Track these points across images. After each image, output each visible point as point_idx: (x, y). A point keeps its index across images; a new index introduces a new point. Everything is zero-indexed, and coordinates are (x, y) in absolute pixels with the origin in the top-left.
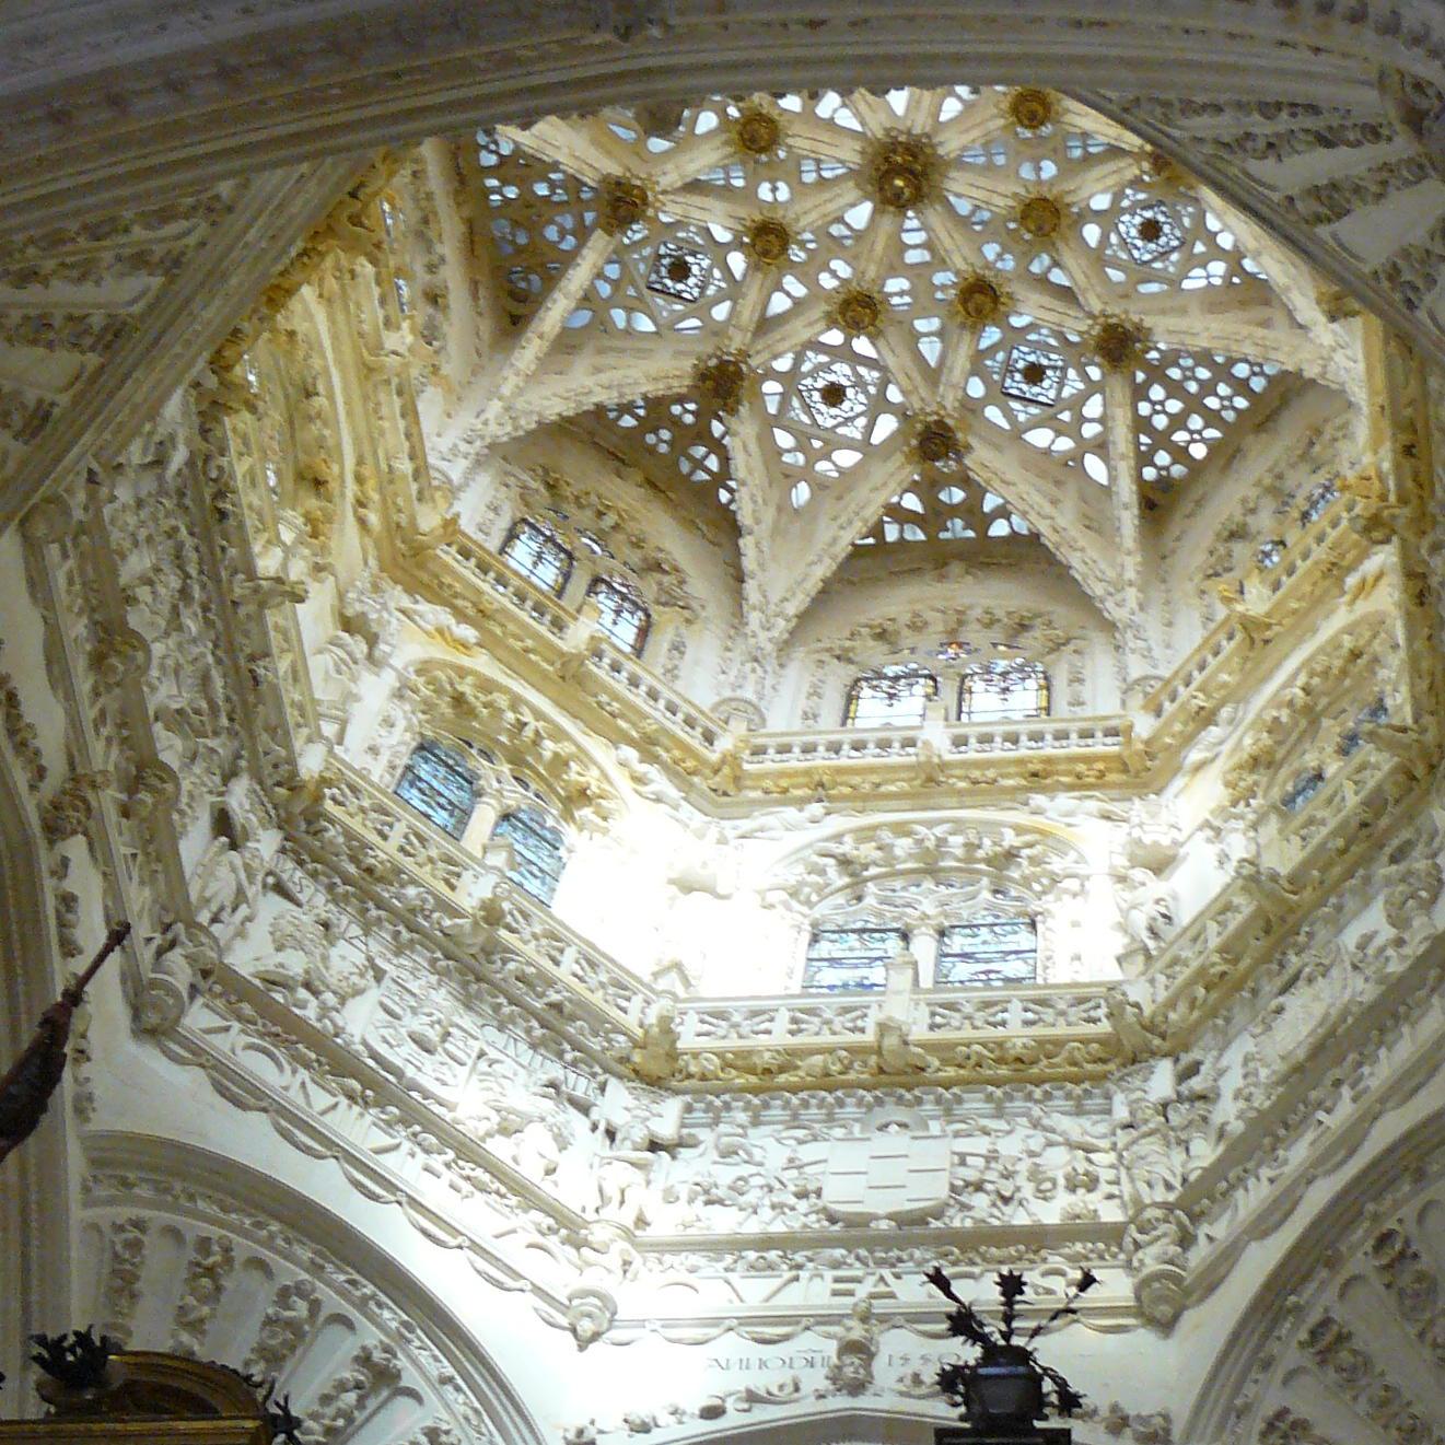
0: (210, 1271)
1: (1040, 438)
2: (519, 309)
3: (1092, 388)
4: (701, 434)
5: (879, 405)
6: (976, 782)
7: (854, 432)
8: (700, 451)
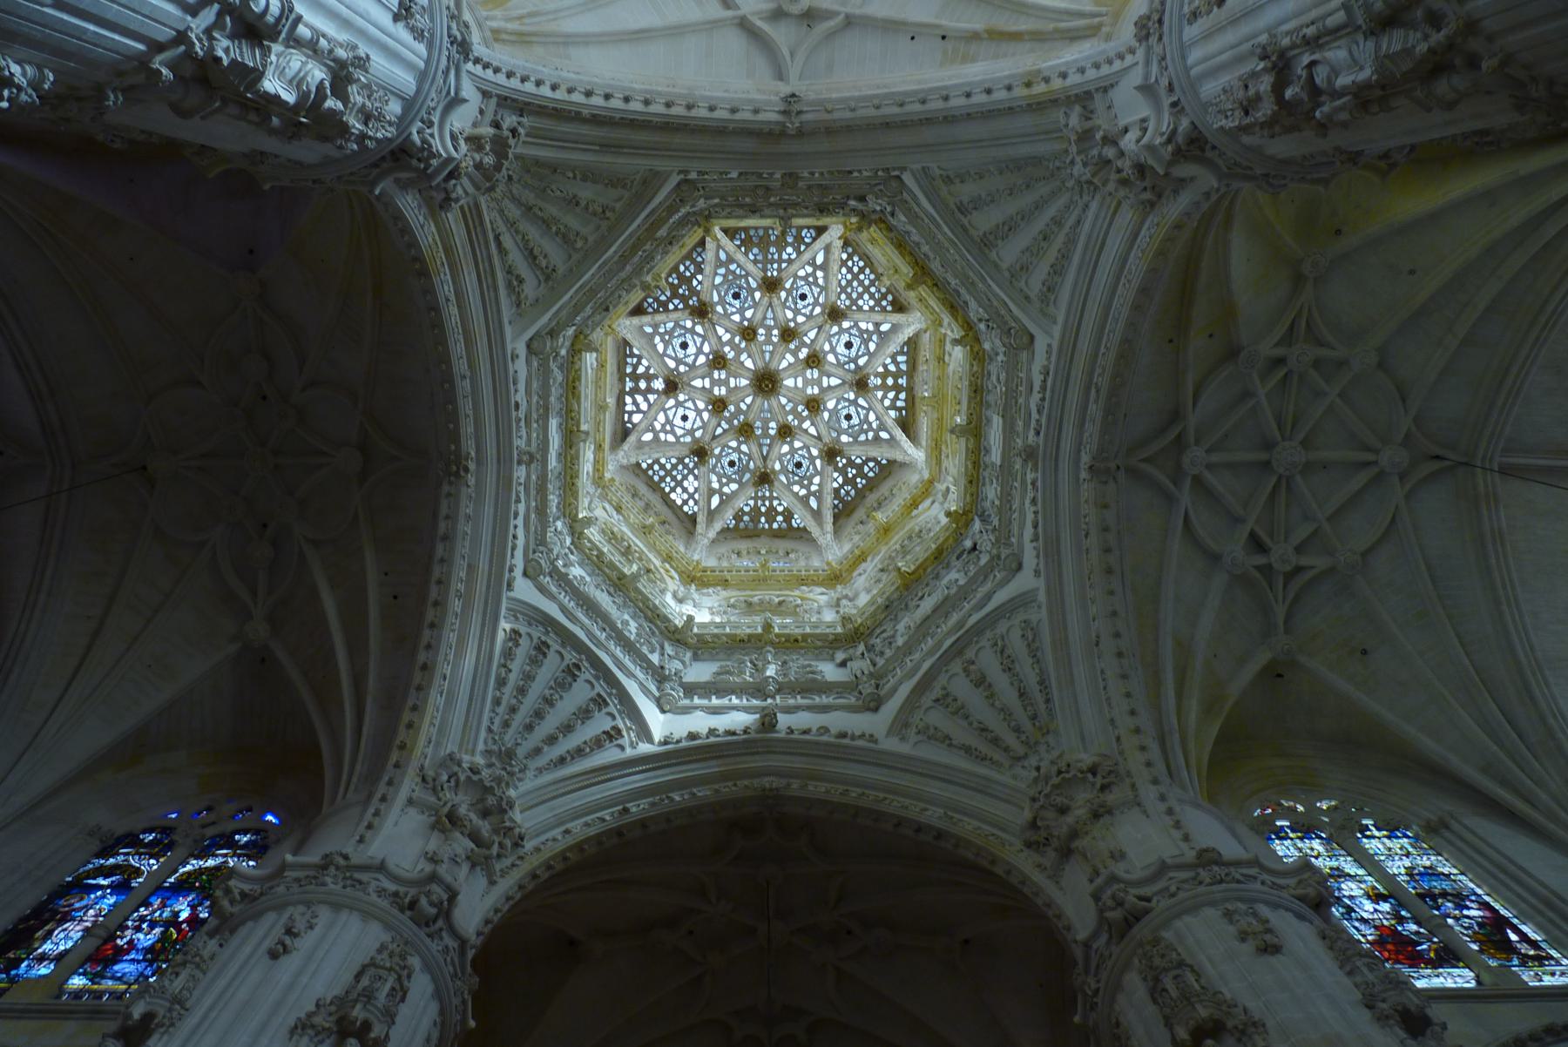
0: (604, 212)
1: (661, 418)
2: (729, 233)
3: (677, 438)
4: (675, 295)
5: (679, 361)
6: (599, 424)
7: (670, 351)
8: (668, 294)
